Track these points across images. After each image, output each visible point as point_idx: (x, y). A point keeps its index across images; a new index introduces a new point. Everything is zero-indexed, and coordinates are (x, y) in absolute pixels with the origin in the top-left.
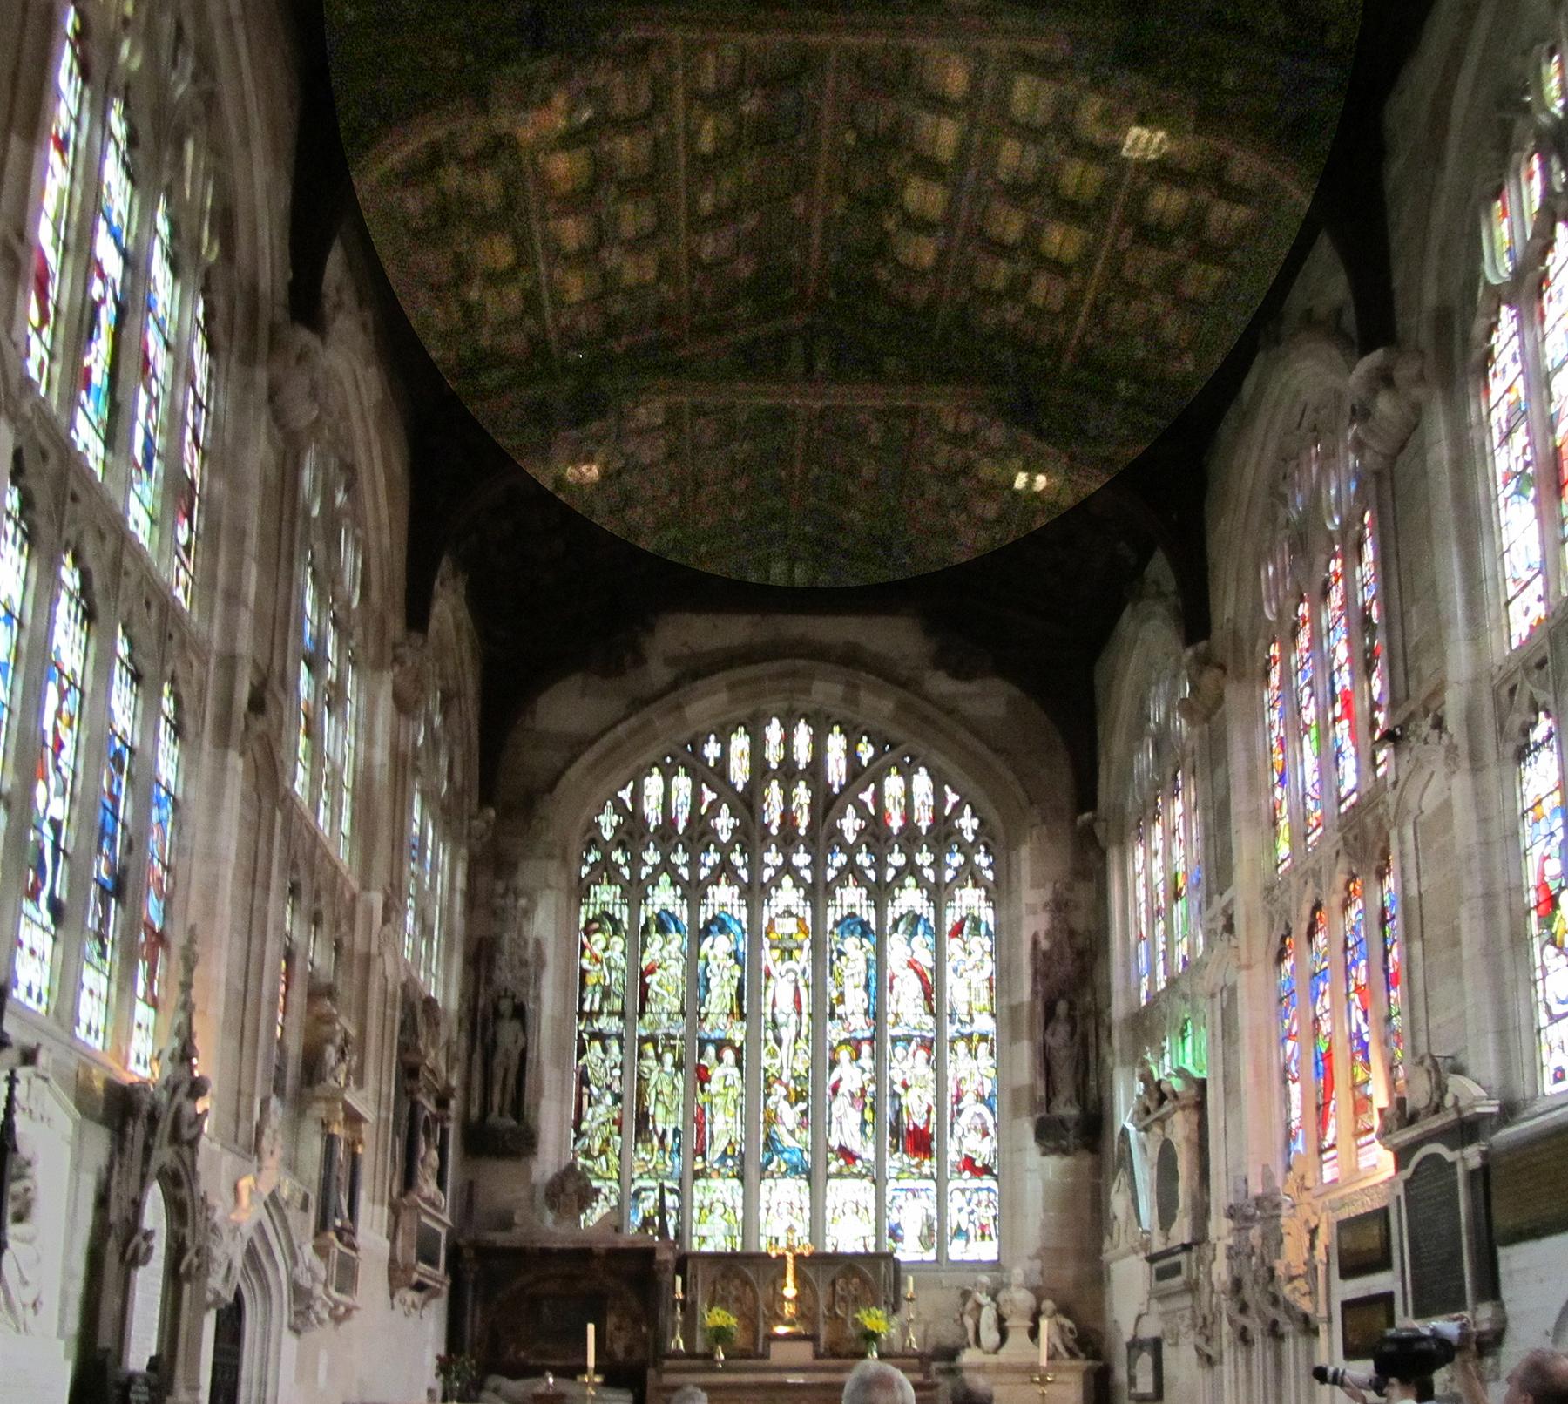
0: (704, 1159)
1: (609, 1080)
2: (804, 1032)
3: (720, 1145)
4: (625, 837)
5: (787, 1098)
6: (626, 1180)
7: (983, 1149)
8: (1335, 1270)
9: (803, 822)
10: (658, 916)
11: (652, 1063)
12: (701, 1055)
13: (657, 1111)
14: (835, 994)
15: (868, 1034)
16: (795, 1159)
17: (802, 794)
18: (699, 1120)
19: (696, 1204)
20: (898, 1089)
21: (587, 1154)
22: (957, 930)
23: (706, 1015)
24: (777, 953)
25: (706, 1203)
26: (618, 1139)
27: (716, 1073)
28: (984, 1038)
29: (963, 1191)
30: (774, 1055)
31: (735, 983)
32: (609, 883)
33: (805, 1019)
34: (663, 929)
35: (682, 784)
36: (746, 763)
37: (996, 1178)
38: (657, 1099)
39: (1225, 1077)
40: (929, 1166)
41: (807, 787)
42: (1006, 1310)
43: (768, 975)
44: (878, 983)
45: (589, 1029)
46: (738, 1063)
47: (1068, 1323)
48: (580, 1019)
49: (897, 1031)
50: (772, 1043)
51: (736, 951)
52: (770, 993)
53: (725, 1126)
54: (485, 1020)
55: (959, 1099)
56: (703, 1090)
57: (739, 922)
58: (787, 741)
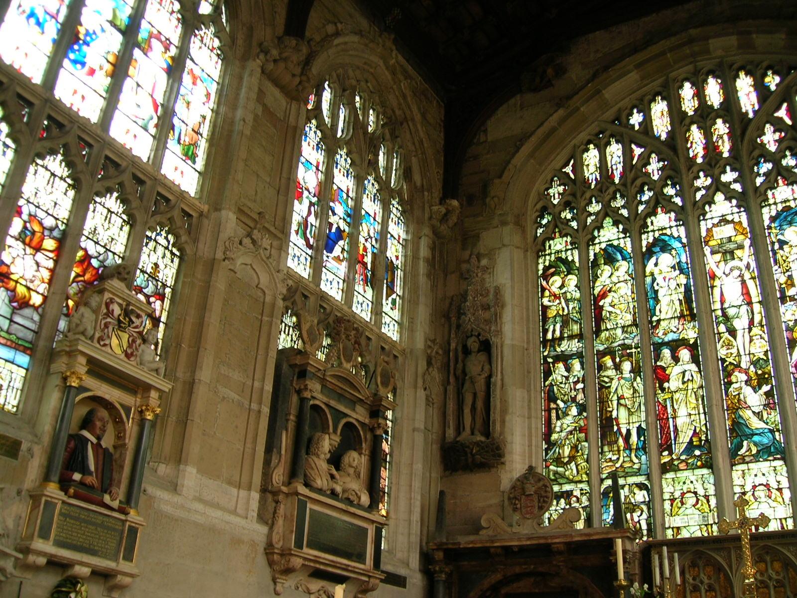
0: (671, 453)
1: (573, 393)
2: (757, 318)
3: (685, 437)
4: (570, 198)
5: (748, 382)
6: (595, 481)
9: (725, 148)
10: (605, 250)
11: (611, 373)
12: (658, 357)
13: (623, 415)
14: (783, 279)
16: (765, 441)
17: (721, 127)
18: (661, 417)
19: (666, 496)
21: (558, 461)
23: (659, 321)
24: (718, 257)
25: (677, 494)
26: (586, 444)
27: (675, 372)
30: (729, 345)
31: (682, 289)
32: (561, 236)
33: (757, 308)
34: (610, 260)
35: (615, 150)
36: (667, 120)
38: (619, 404)
41: (724, 122)
43: (713, 277)
45: (553, 353)
46: (695, 359)
48: (545, 347)
51: (679, 263)
52: (717, 292)
53: (687, 419)
56: (663, 390)
57: (679, 239)
58: (700, 94)
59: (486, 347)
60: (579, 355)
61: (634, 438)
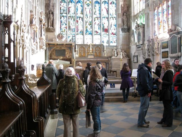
1: (65, 22)
2: (91, 16)
5: (89, 24)
7: (114, 32)
8: (161, 48)
12: (77, 19)
14: (95, 11)
15: (99, 16)
20: (103, 24)
21: (62, 31)
22: (111, 3)
27: (79, 21)
28: (114, 17)
29: (112, 37)
31: (81, 9)
37: (116, 35)
39: (147, 24)
40: (107, 34)
42: (118, 52)
43: (86, 9)
44: (100, 10)
46: (82, 20)
47: (126, 53)
49: (104, 16)
50: (86, 17)
53: (80, 28)
54: (48, 14)
55: (111, 25)
57: (82, 1)
59: (53, 13)
60: (66, 16)
61: (73, 30)
